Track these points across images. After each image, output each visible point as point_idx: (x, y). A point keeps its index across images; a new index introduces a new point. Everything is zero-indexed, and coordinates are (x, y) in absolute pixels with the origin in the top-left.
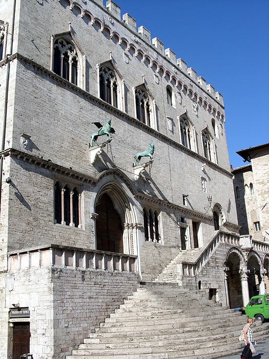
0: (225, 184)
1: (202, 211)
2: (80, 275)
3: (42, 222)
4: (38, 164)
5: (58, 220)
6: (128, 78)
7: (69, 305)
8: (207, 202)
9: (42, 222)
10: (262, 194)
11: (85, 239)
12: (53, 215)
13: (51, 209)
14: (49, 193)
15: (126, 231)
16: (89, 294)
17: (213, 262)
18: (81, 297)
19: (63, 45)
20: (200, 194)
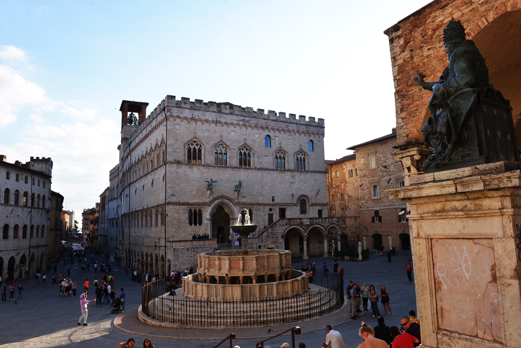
0: (316, 180)
1: (288, 202)
2: (186, 249)
3: (182, 227)
4: (179, 205)
5: (191, 224)
6: (234, 145)
7: (181, 260)
9: (182, 227)
10: (360, 177)
11: (204, 230)
12: (188, 222)
13: (187, 221)
14: (185, 215)
15: (231, 221)
16: (190, 255)
17: (271, 235)
18: (187, 257)
19: (192, 144)
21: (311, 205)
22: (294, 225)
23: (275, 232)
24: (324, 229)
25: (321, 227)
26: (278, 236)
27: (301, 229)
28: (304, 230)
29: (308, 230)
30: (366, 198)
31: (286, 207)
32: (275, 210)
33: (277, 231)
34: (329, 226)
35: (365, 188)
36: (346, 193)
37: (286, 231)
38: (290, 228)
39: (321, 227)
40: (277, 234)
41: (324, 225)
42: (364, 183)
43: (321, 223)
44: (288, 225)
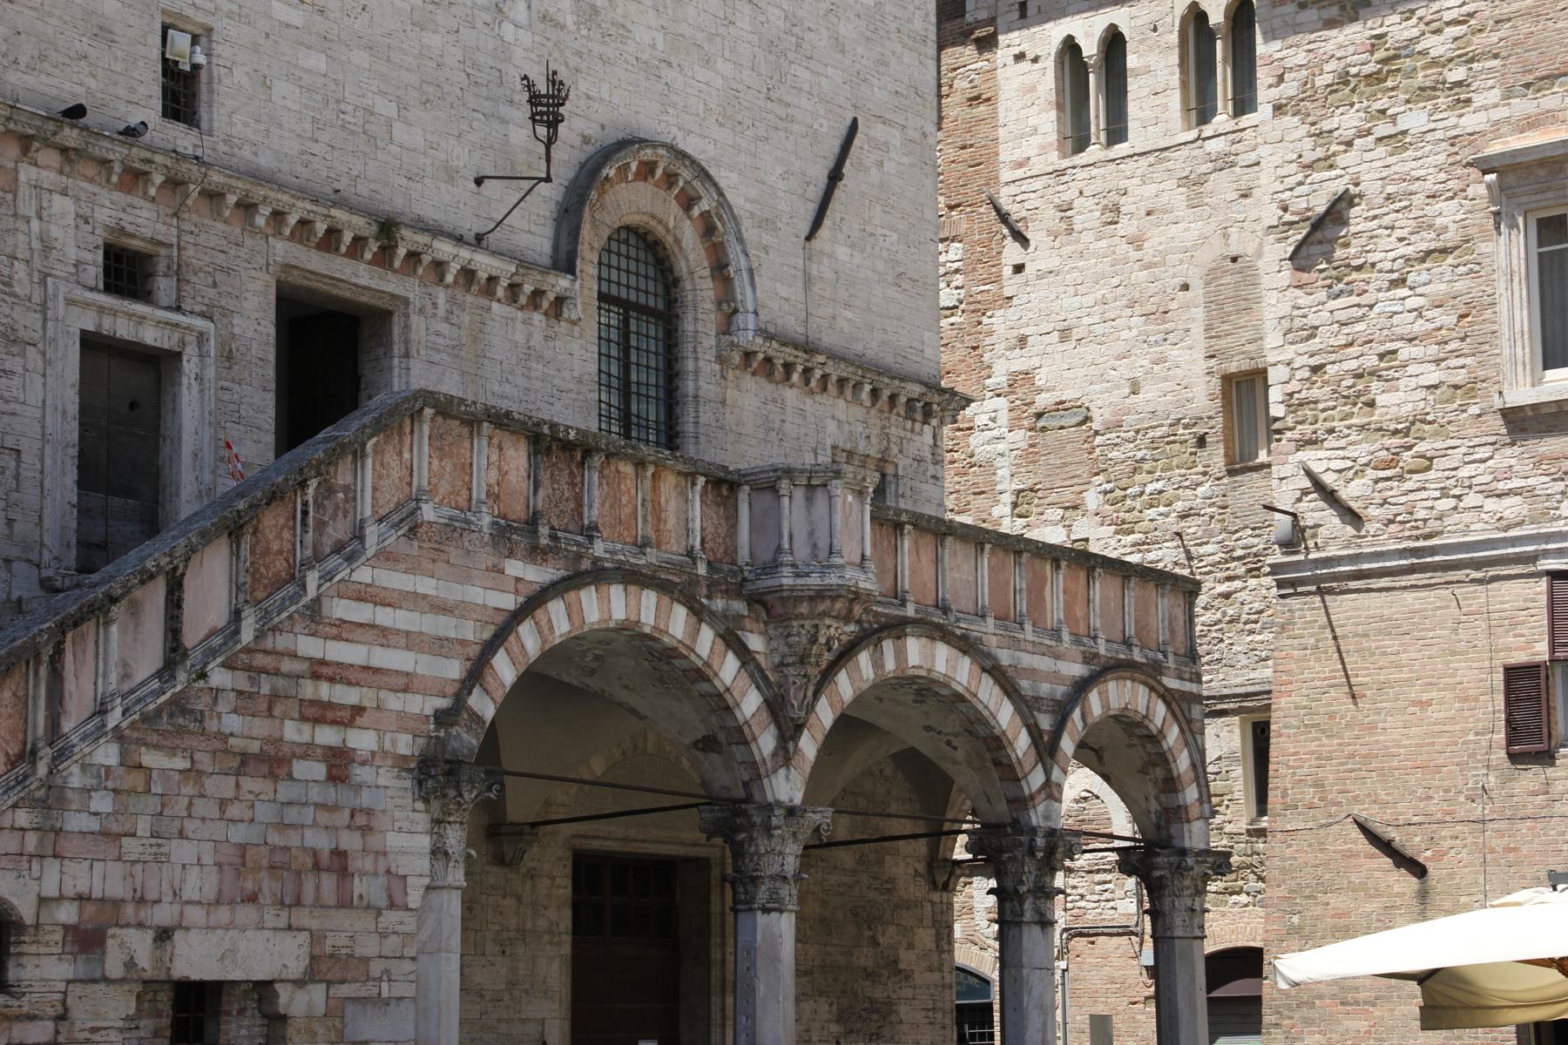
8: (521, 135)
20: (434, 41)
21: (748, 355)
22: (633, 577)
23: (309, 646)
24: (1022, 743)
25: (988, 694)
26: (361, 740)
27: (729, 669)
28: (775, 706)
29: (825, 714)
30: (1395, 402)
31: (391, 284)
32: (200, 290)
33: (343, 630)
34: (1081, 687)
35: (1387, 251)
36: (999, 378)
37: (505, 670)
38: (558, 619)
39: (988, 694)
40: (348, 696)
41: (1027, 660)
42: (1370, 187)
43: (988, 631)
44: (536, 553)
